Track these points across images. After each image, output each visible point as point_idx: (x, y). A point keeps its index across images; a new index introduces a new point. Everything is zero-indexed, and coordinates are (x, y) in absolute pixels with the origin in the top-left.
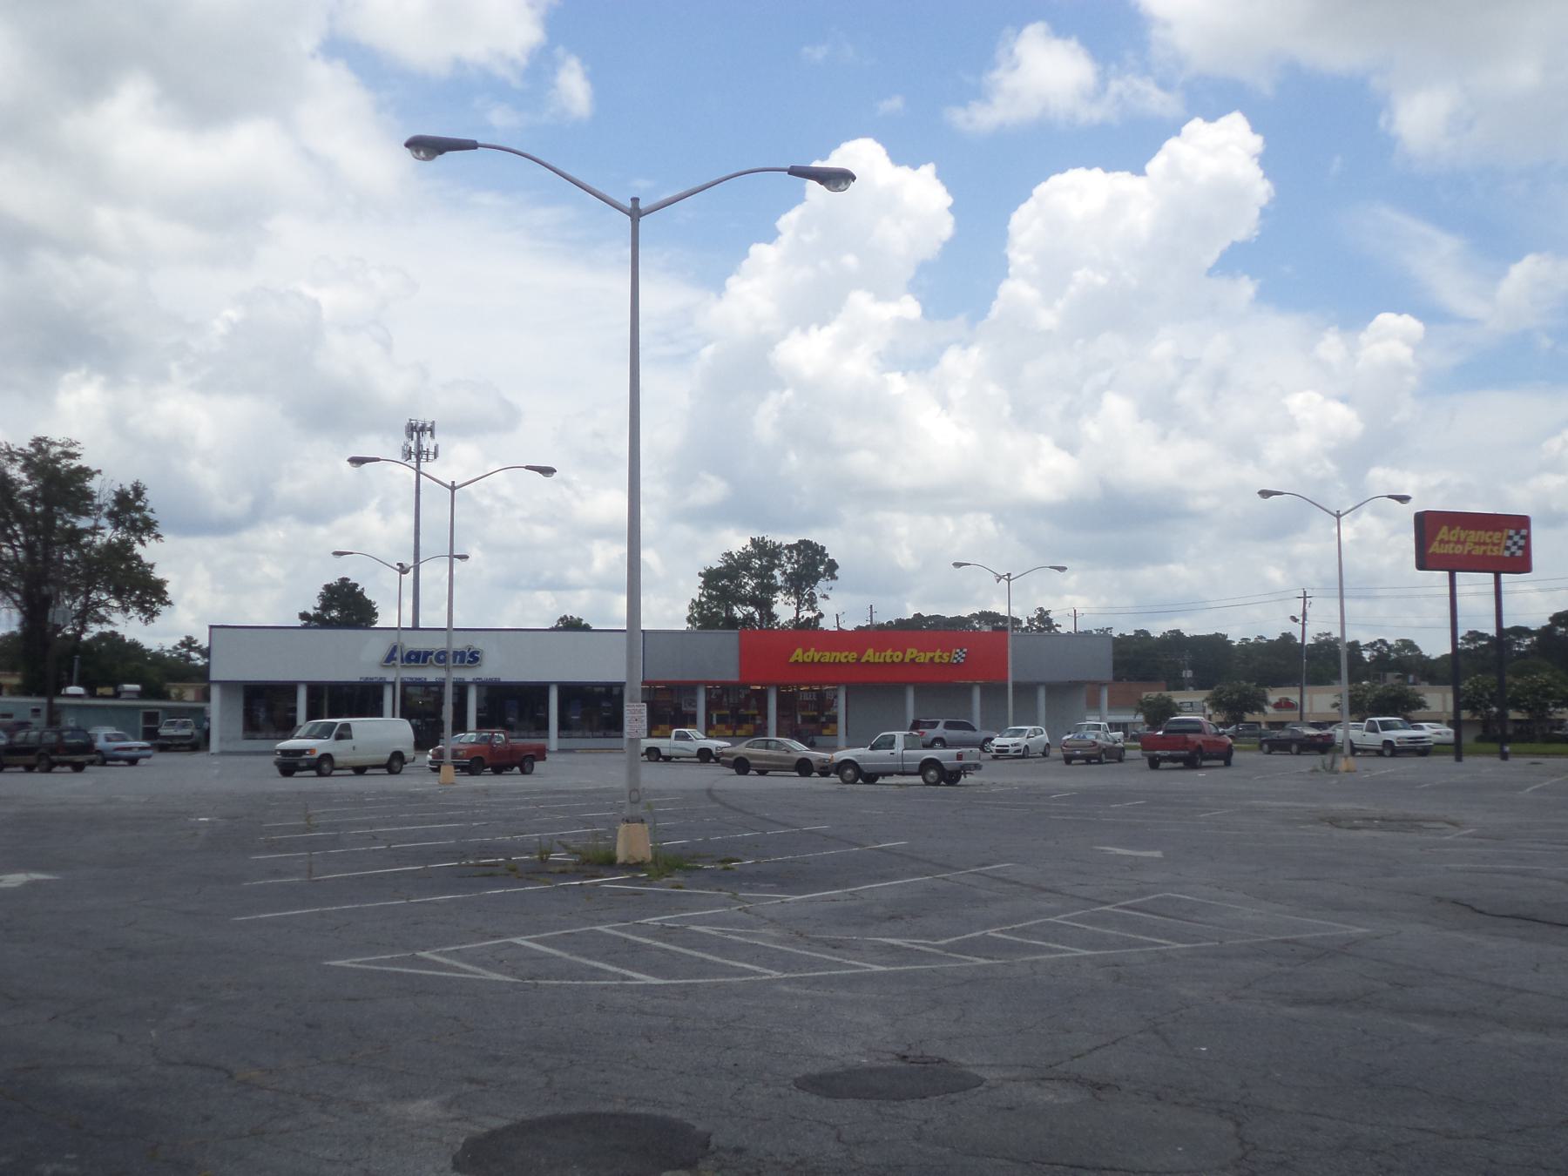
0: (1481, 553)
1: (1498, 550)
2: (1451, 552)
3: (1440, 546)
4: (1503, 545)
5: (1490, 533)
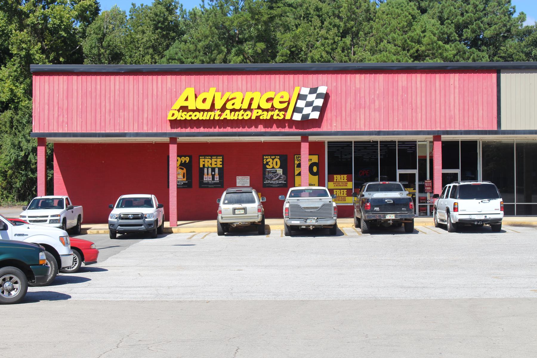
0: (269, 118)
2: (240, 118)
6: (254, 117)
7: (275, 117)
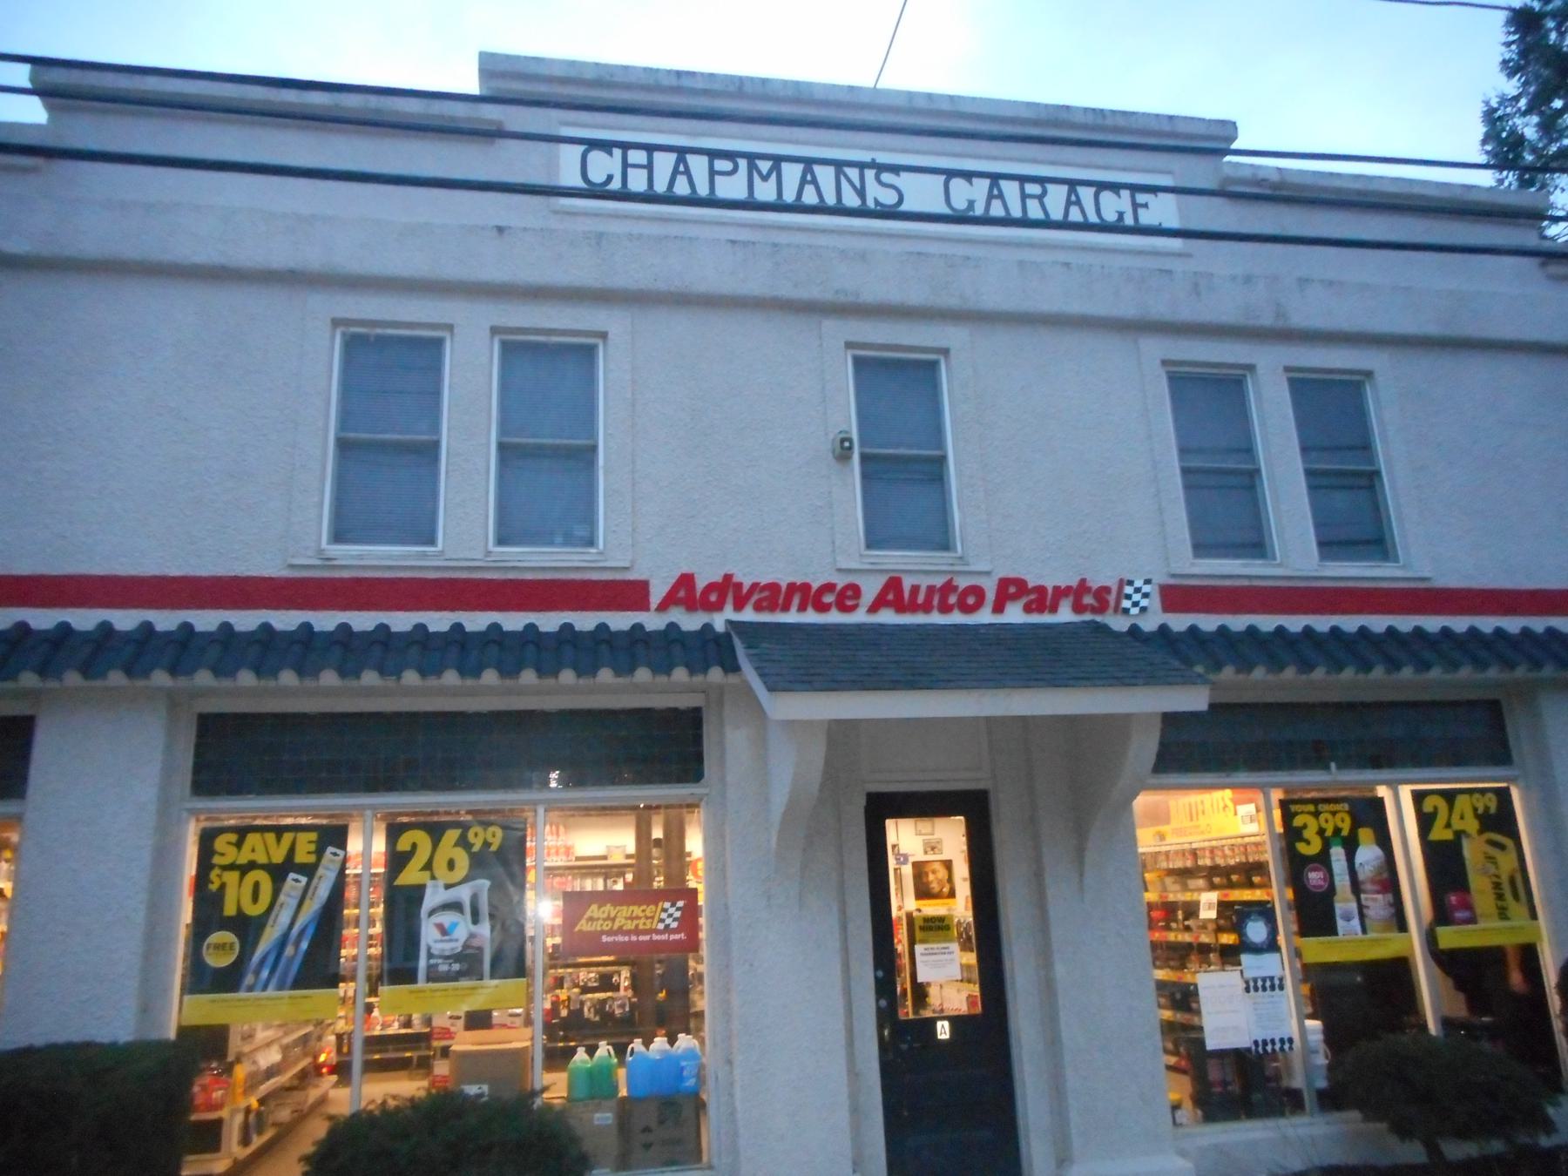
0: (633, 927)
1: (652, 923)
3: (587, 923)
4: (656, 919)
5: (644, 907)
6: (615, 927)
7: (641, 927)
